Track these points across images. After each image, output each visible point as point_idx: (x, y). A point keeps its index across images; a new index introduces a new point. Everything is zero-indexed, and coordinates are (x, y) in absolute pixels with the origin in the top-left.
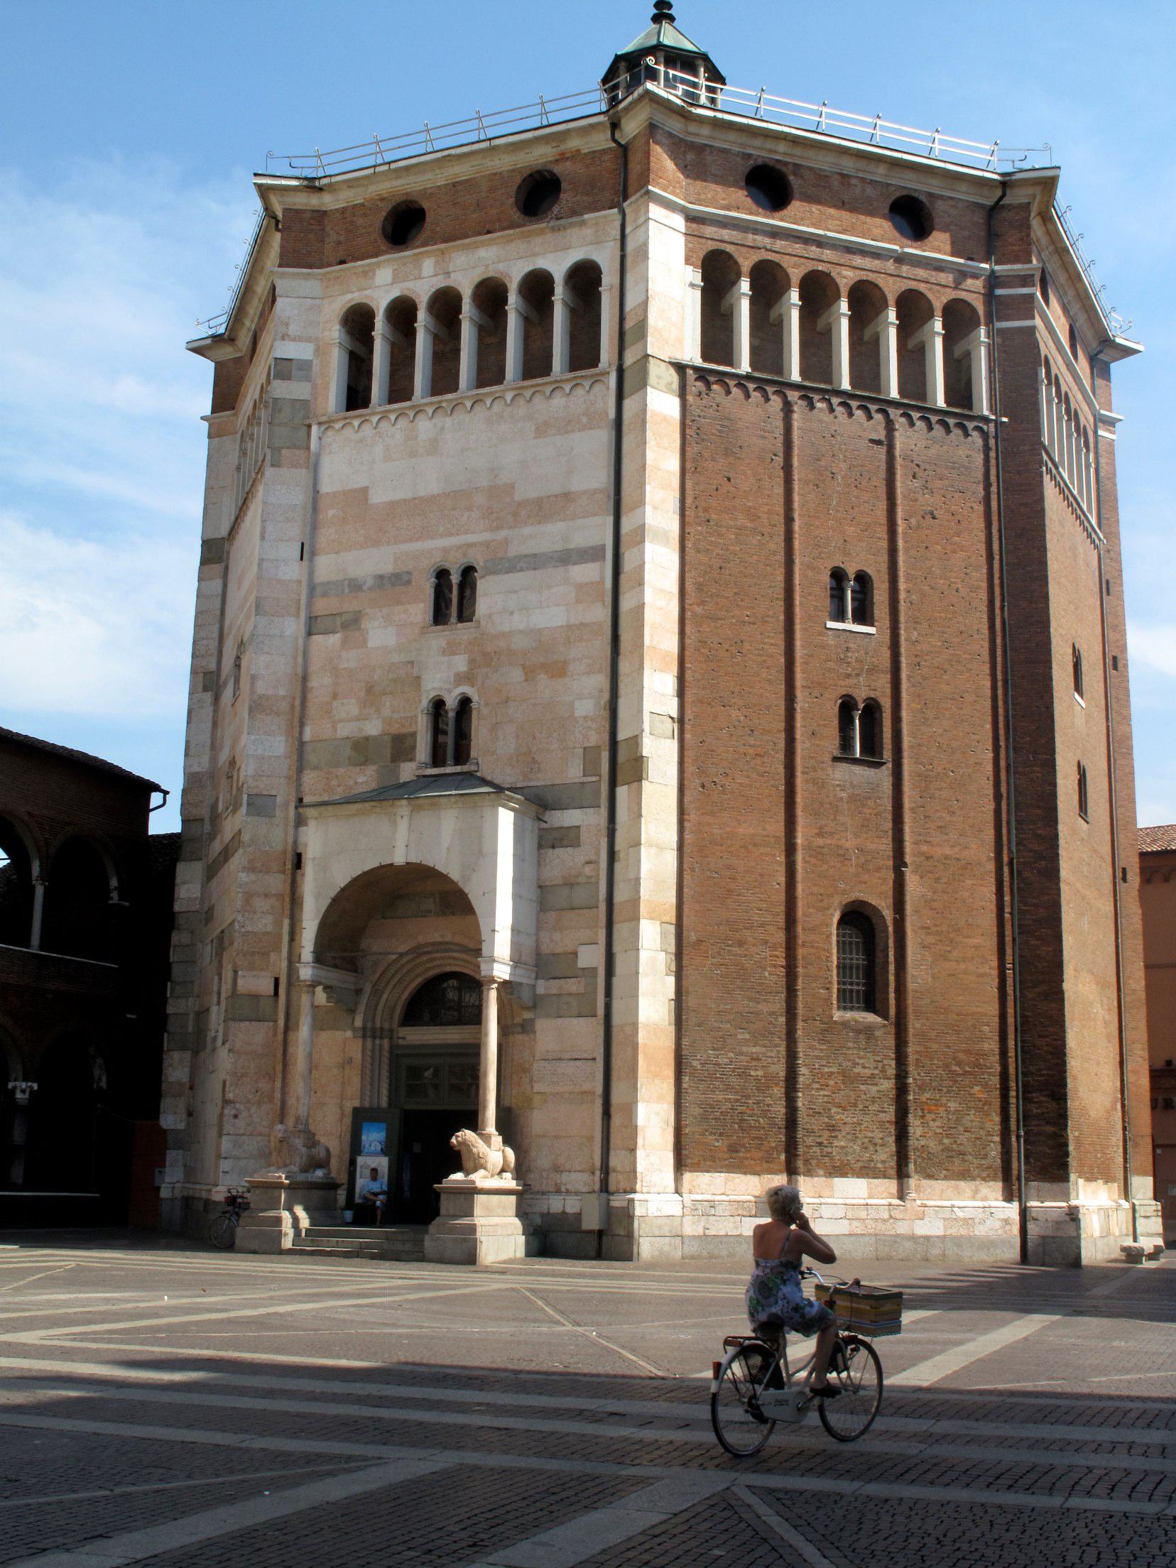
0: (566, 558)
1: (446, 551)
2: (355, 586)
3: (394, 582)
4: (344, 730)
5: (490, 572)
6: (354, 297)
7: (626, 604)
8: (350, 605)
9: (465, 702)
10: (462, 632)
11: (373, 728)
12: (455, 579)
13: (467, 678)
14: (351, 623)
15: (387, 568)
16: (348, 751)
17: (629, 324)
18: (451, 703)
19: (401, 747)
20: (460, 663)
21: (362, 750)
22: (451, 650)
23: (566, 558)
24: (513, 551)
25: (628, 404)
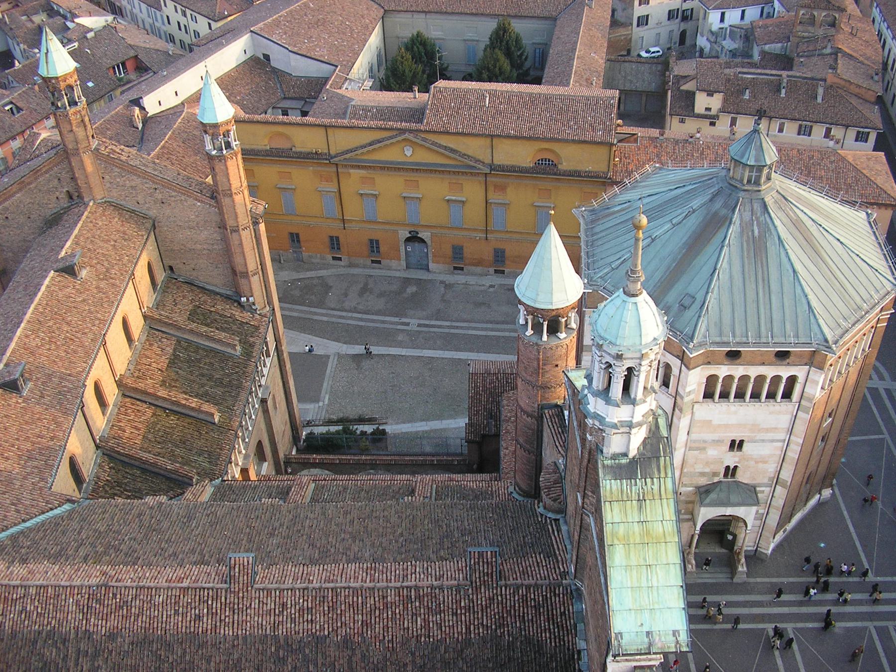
0: (772, 441)
1: (736, 436)
2: (705, 442)
3: (718, 442)
4: (697, 471)
5: (748, 442)
6: (712, 373)
7: (788, 453)
8: (704, 445)
9: (736, 467)
10: (739, 453)
11: (707, 470)
12: (737, 442)
13: (738, 463)
14: (703, 449)
15: (717, 439)
16: (697, 474)
17: (804, 394)
18: (732, 467)
19: (715, 474)
20: (737, 459)
21: (702, 474)
22: (734, 456)
23: (772, 441)
24: (757, 438)
25: (799, 412)
